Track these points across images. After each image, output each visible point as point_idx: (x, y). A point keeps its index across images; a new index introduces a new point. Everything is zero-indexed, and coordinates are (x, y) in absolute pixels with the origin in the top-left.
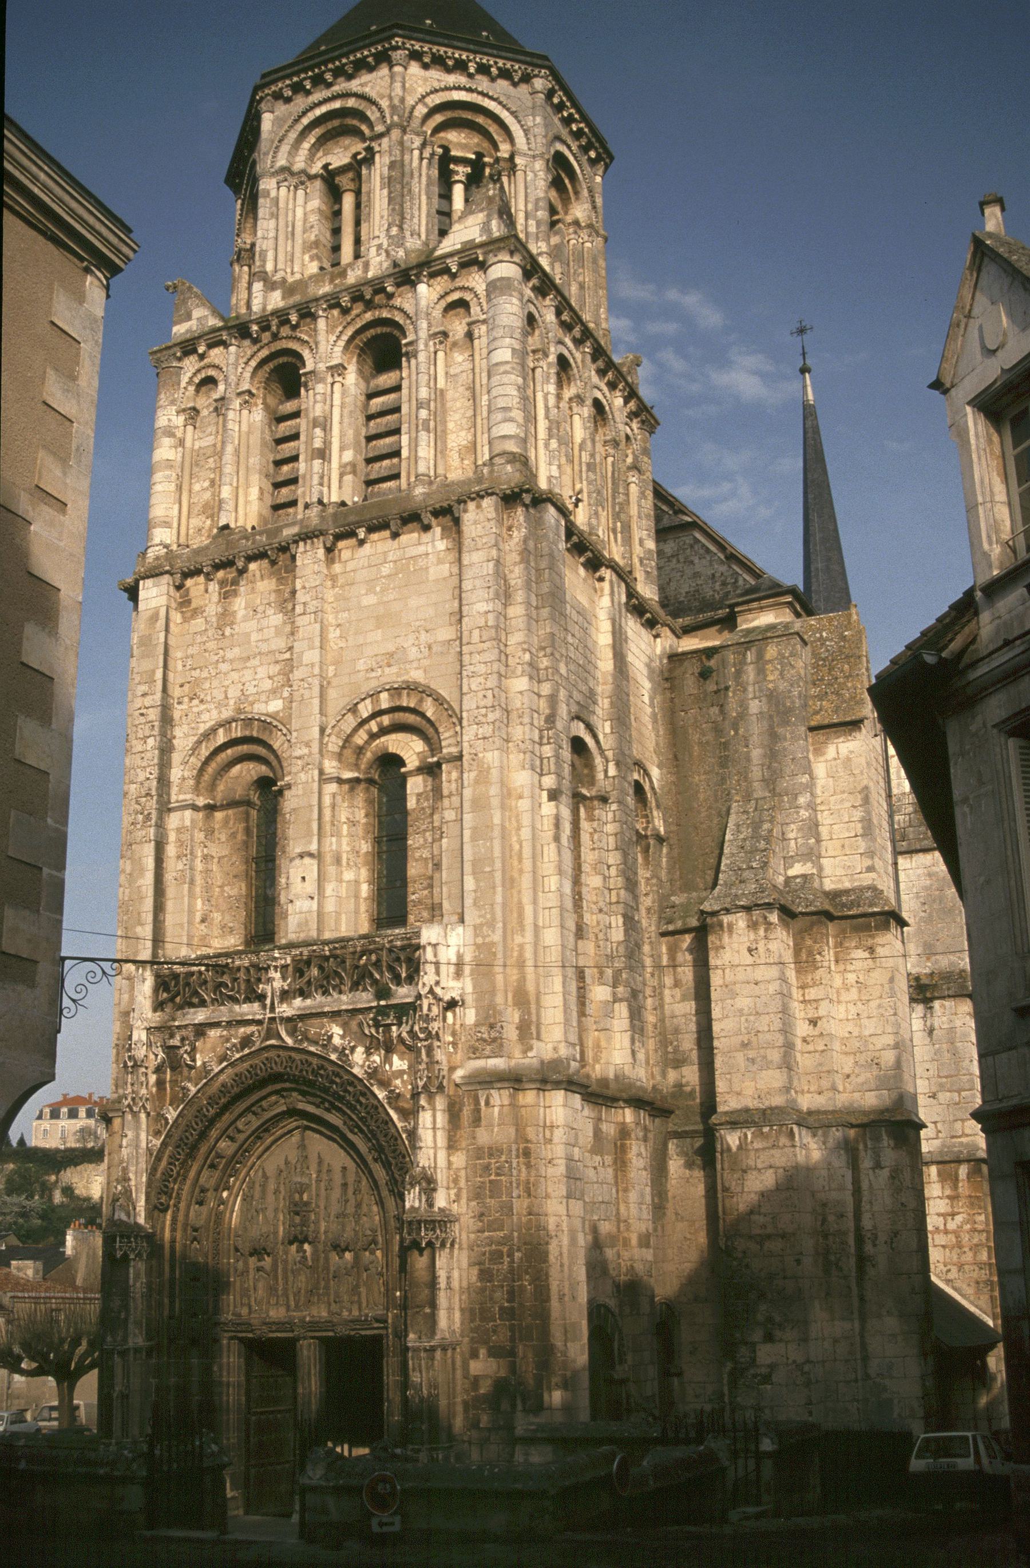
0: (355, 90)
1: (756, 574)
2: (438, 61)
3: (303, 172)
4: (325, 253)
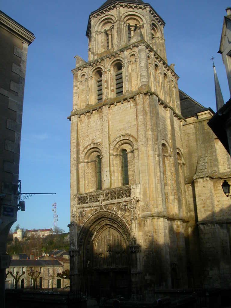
0: (109, 14)
2: (126, 6)
3: (100, 31)
4: (106, 47)
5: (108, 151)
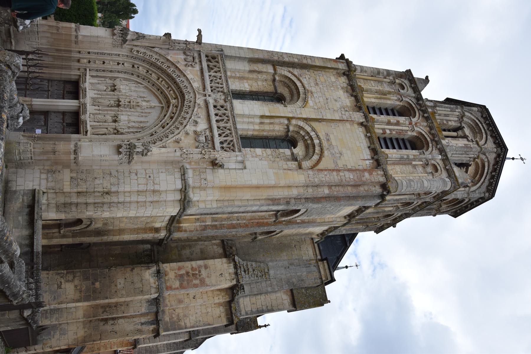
3: (463, 120)
5: (296, 116)
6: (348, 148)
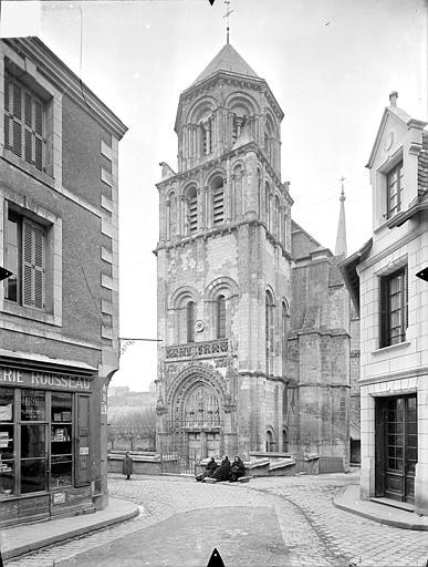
1: (318, 245)
6: (224, 255)
